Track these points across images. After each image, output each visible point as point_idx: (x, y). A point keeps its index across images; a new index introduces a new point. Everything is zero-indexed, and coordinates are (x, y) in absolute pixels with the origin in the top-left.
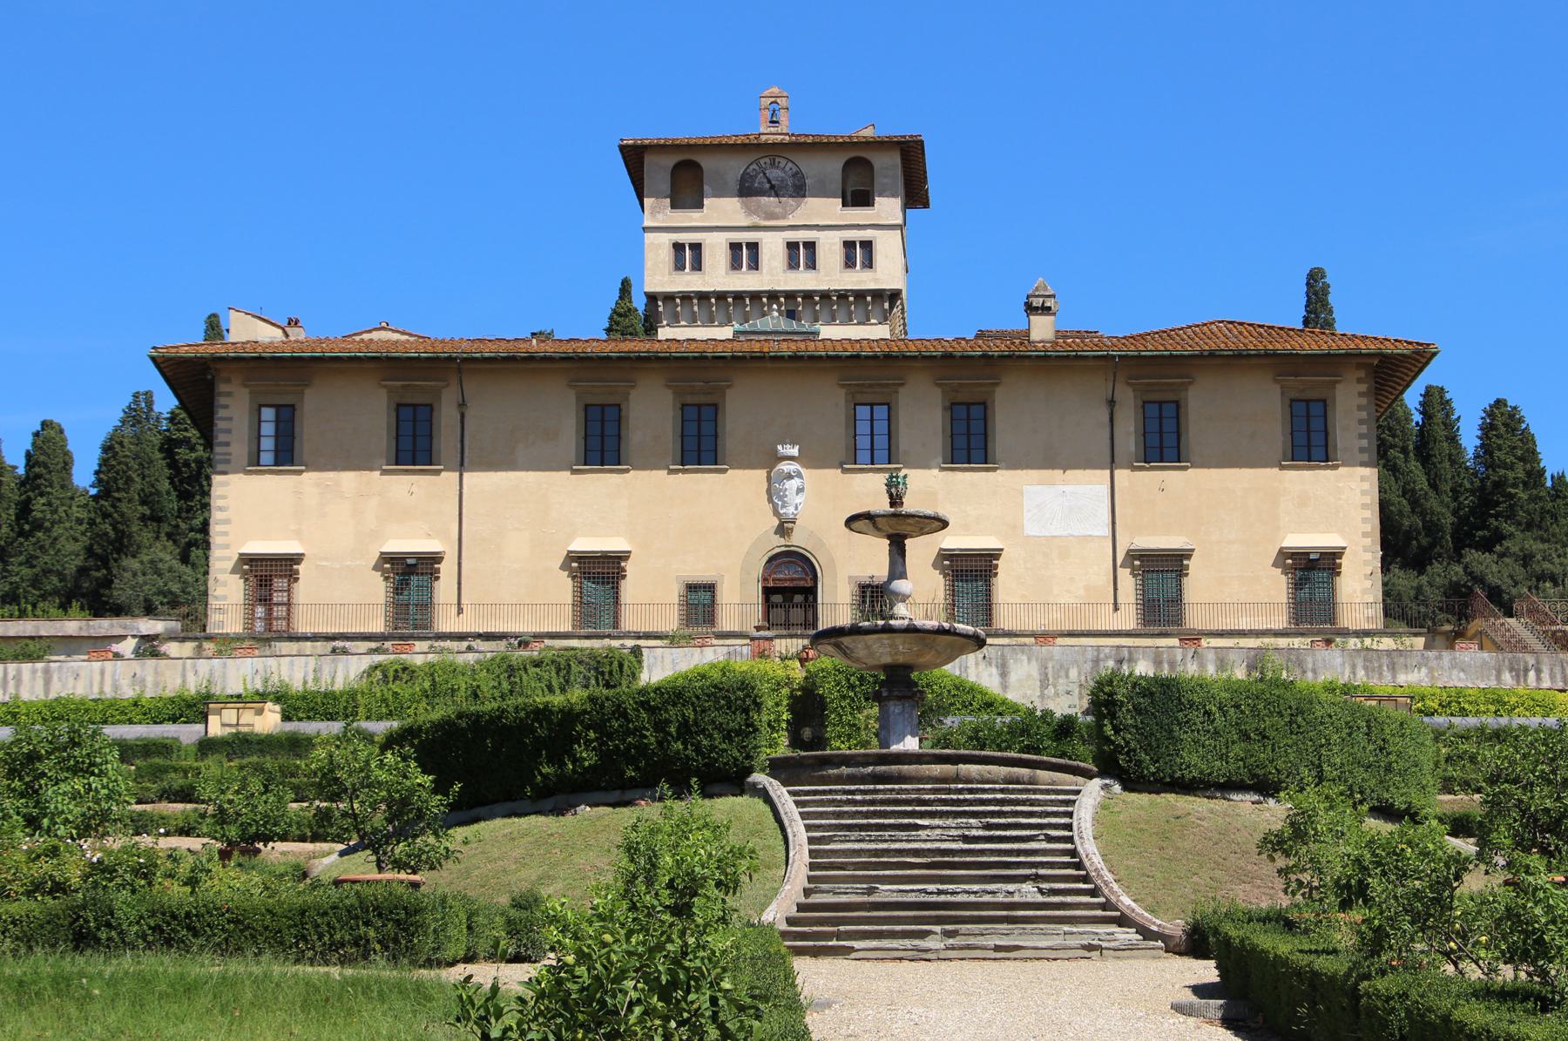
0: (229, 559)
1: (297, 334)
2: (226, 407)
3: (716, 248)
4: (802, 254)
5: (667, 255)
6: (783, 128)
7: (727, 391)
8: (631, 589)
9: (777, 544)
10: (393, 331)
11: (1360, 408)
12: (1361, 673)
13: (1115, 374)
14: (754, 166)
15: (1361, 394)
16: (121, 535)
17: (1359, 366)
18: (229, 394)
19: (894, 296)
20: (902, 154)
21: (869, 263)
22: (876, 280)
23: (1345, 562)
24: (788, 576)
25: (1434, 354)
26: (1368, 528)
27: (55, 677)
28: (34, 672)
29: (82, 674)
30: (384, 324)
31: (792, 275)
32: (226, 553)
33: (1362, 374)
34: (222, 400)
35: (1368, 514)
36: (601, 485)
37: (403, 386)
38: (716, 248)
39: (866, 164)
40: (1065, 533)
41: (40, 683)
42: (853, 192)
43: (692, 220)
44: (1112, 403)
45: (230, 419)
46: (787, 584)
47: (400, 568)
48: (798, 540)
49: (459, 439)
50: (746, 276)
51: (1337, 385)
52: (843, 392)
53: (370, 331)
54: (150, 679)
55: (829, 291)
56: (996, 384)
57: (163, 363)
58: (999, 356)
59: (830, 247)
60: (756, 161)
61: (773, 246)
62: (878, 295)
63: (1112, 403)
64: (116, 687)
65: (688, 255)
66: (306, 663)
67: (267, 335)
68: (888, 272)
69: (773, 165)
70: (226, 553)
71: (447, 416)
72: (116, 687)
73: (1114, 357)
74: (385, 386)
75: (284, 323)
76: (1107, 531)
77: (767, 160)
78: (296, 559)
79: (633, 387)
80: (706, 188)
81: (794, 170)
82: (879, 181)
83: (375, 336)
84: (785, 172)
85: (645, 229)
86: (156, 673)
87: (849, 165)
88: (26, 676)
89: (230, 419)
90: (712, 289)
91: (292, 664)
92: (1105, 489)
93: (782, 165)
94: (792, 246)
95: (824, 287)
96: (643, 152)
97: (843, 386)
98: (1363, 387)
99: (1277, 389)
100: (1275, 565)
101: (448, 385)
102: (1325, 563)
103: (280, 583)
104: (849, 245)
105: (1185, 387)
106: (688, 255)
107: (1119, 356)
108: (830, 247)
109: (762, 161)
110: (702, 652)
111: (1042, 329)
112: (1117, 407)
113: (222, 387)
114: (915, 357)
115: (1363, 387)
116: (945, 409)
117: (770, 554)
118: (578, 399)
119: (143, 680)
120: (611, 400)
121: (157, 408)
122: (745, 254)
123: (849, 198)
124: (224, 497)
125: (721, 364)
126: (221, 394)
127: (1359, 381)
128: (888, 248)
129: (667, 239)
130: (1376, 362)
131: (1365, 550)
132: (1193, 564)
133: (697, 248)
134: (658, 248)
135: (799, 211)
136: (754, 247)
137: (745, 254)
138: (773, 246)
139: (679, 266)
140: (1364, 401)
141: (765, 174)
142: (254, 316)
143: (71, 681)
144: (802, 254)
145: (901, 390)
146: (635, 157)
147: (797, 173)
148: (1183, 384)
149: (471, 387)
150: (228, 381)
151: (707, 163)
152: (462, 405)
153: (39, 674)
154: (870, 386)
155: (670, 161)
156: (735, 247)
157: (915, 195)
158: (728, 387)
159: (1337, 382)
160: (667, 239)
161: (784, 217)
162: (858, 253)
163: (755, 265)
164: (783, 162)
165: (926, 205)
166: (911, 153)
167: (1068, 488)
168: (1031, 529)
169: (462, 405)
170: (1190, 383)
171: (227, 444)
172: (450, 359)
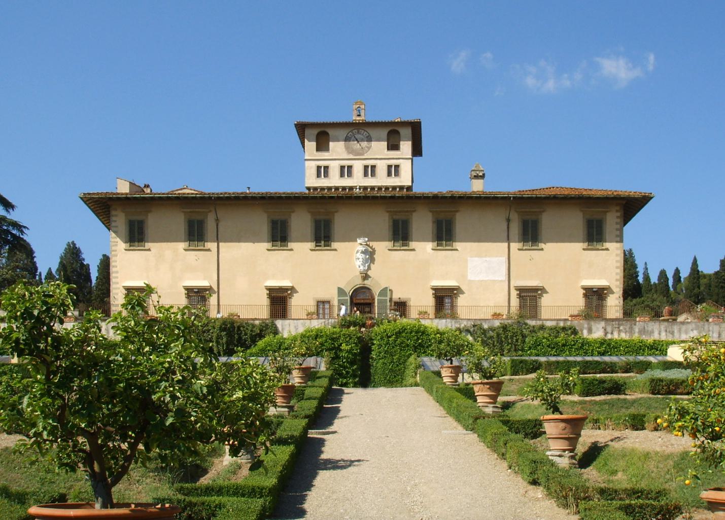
2: (115, 221)
4: (370, 171)
5: (314, 171)
6: (362, 118)
7: (336, 214)
9: (358, 282)
10: (191, 190)
11: (617, 223)
12: (663, 334)
13: (510, 210)
14: (350, 133)
15: (618, 217)
17: (617, 205)
18: (116, 216)
19: (409, 188)
20: (412, 129)
22: (401, 182)
24: (361, 298)
25: (652, 198)
30: (185, 187)
31: (366, 179)
33: (618, 208)
34: (113, 218)
36: (280, 256)
37: (190, 212)
39: (397, 133)
40: (487, 279)
42: (392, 145)
43: (324, 156)
44: (508, 220)
45: (116, 227)
46: (362, 301)
48: (367, 283)
49: (216, 235)
50: (347, 180)
51: (607, 213)
52: (387, 214)
53: (181, 189)
55: (382, 186)
56: (457, 211)
57: (87, 201)
58: (459, 197)
59: (382, 167)
61: (358, 167)
62: (401, 188)
65: (322, 171)
69: (358, 133)
73: (511, 197)
74: (183, 212)
75: (142, 186)
77: (356, 131)
79: (293, 212)
81: (367, 134)
84: (364, 136)
85: (306, 160)
89: (116, 227)
90: (333, 185)
92: (504, 259)
93: (362, 133)
94: (366, 167)
95: (380, 184)
96: (304, 128)
97: (388, 212)
98: (619, 214)
101: (210, 211)
105: (541, 212)
107: (513, 197)
108: (382, 167)
109: (354, 131)
110: (311, 322)
111: (477, 186)
112: (510, 223)
113: (113, 213)
114: (421, 197)
115: (619, 214)
116: (434, 222)
117: (354, 288)
118: (268, 217)
122: (347, 171)
123: (390, 147)
126: (112, 216)
127: (617, 211)
130: (624, 202)
133: (326, 168)
134: (310, 168)
135: (369, 152)
136: (350, 167)
138: (358, 167)
139: (319, 175)
140: (619, 220)
141: (355, 137)
144: (370, 171)
145: (414, 214)
146: (302, 129)
147: (368, 136)
148: (540, 212)
149: (221, 213)
150: (116, 210)
151: (331, 132)
152: (217, 220)
154: (400, 212)
155: (315, 132)
157: (417, 151)
158: (336, 212)
159: (607, 212)
160: (314, 164)
161: (363, 155)
162: (393, 170)
164: (363, 131)
165: (421, 155)
166: (416, 129)
167: (488, 259)
169: (217, 220)
170: (543, 211)
172: (210, 198)
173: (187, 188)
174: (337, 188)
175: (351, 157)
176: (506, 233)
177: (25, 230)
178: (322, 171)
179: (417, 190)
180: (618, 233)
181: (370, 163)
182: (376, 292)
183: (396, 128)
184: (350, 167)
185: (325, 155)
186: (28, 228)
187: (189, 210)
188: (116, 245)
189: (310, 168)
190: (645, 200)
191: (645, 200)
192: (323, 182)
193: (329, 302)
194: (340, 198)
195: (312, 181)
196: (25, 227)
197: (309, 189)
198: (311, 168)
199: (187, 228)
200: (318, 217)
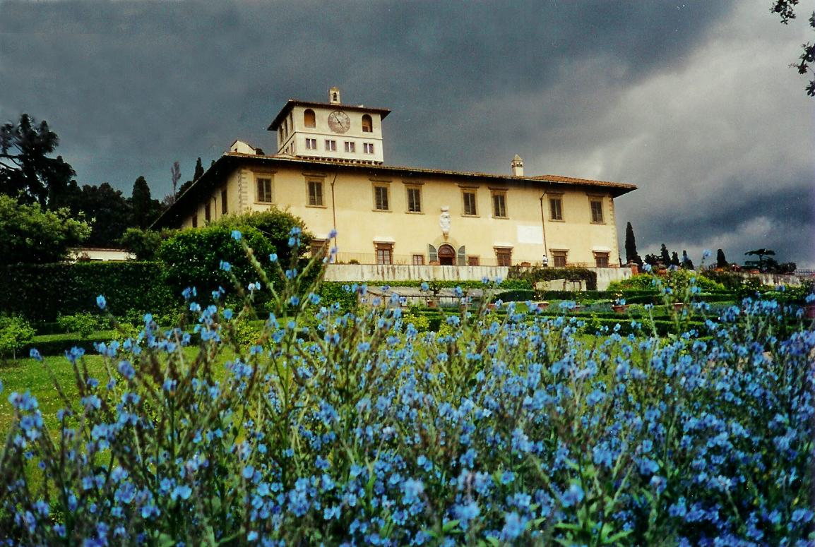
4: (350, 146)
5: (304, 142)
9: (442, 242)
19: (381, 163)
28: (388, 269)
35: (615, 240)
44: (541, 199)
48: (449, 242)
54: (431, 274)
63: (541, 199)
76: (542, 242)
80: (316, 120)
88: (385, 271)
120: (384, 186)
137: (331, 144)
143: (402, 272)
151: (317, 112)
152: (332, 185)
161: (343, 133)
168: (520, 241)
169: (332, 185)
171: (246, 193)
175: (334, 133)
178: (312, 143)
179: (385, 166)
181: (350, 140)
184: (333, 142)
185: (313, 130)
189: (300, 139)
193: (422, 256)
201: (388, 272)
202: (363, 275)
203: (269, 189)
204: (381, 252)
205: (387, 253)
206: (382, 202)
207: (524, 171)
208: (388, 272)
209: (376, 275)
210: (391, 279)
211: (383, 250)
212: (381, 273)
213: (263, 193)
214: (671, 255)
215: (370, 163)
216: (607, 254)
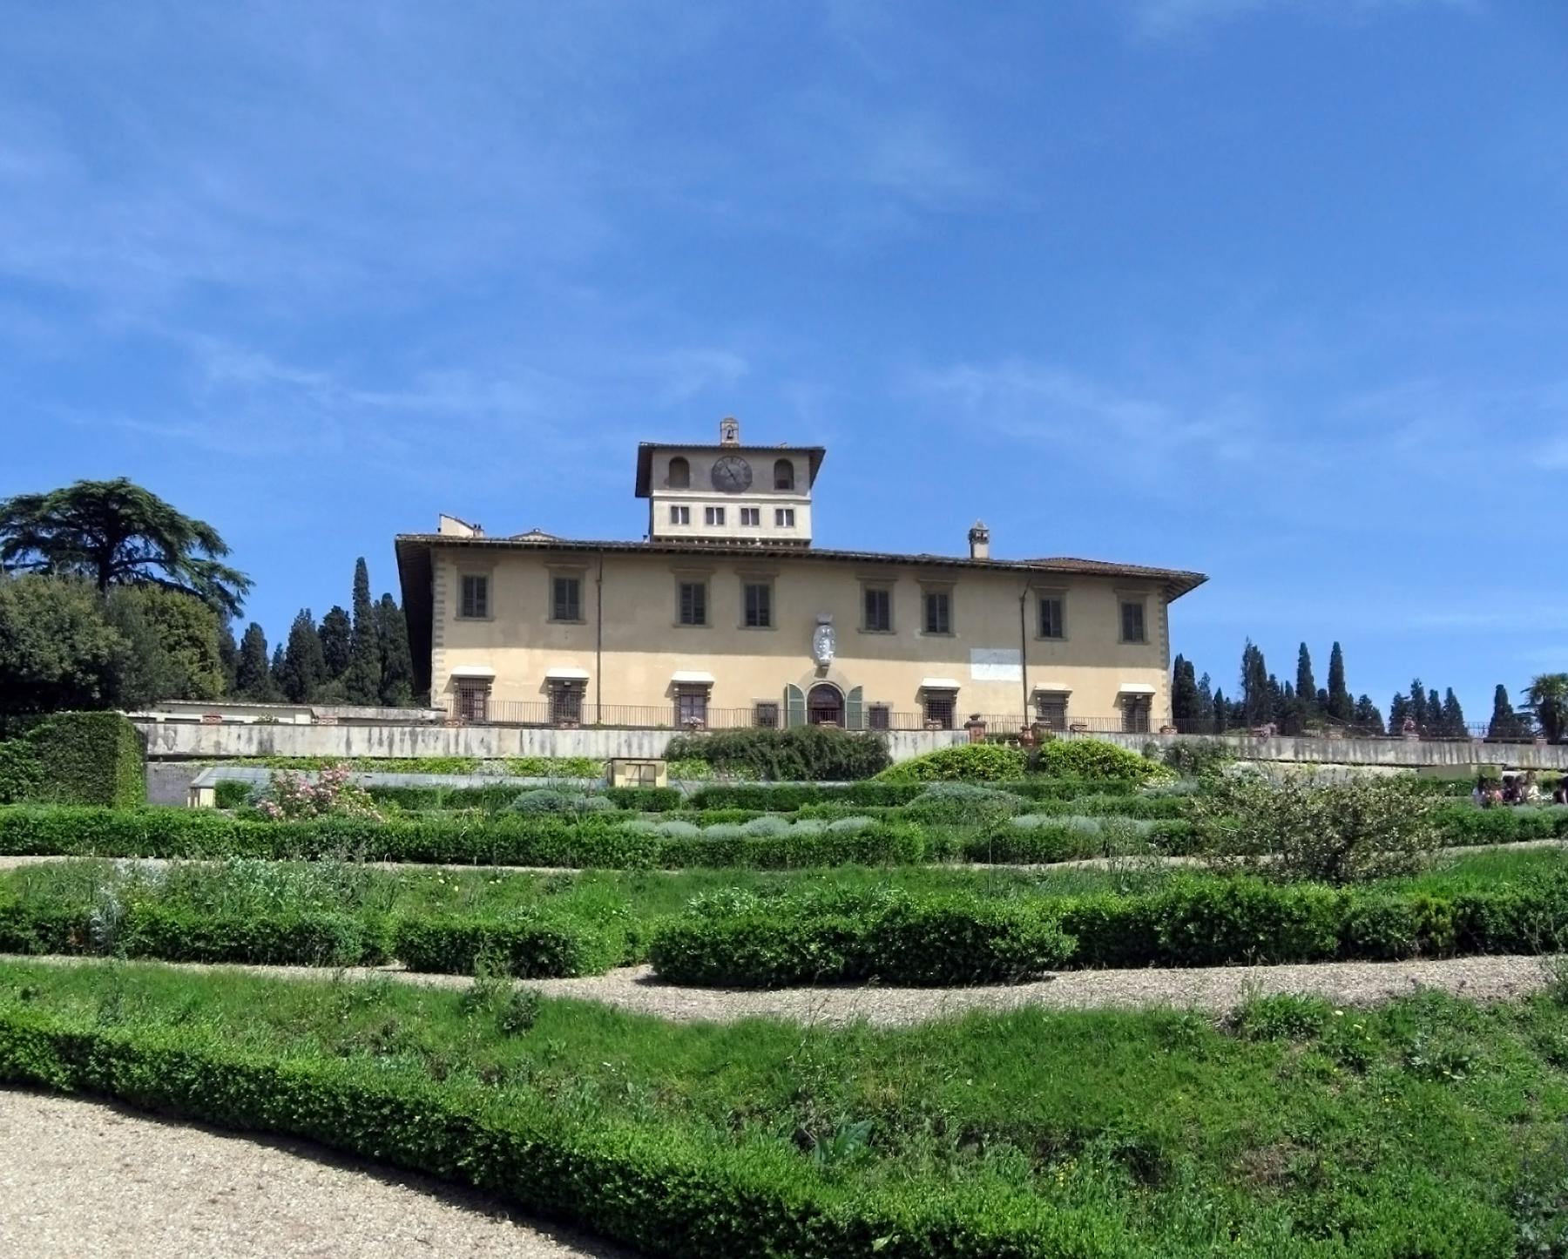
0: (444, 678)
1: (481, 535)
2: (442, 577)
3: (698, 510)
8: (711, 705)
16: (302, 683)
18: (444, 569)
19: (807, 543)
21: (791, 522)
23: (1154, 701)
26: (1165, 682)
27: (420, 738)
28: (403, 734)
29: (441, 737)
32: (443, 673)
38: (698, 510)
41: (408, 743)
45: (444, 586)
47: (558, 688)
54: (494, 745)
59: (767, 512)
60: (722, 459)
61: (733, 511)
62: (797, 542)
64: (467, 747)
66: (619, 736)
67: (464, 533)
68: (802, 529)
70: (443, 673)
71: (588, 590)
72: (467, 747)
76: (1019, 678)
78: (488, 680)
80: (691, 474)
82: (797, 474)
83: (532, 538)
86: (500, 740)
87: (779, 464)
88: (397, 738)
91: (607, 737)
95: (765, 536)
99: (1115, 597)
100: (1115, 706)
102: (1143, 702)
103: (479, 696)
104: (779, 512)
106: (680, 514)
108: (767, 512)
119: (489, 744)
120: (700, 581)
121: (313, 618)
124: (440, 637)
125: (772, 560)
128: (803, 514)
129: (667, 505)
130: (1167, 583)
131: (1164, 694)
132: (1071, 700)
136: (721, 511)
137: (715, 515)
138: (733, 511)
142: (456, 520)
144: (751, 516)
150: (443, 560)
151: (692, 460)
152: (599, 581)
153: (407, 737)
155: (669, 457)
156: (709, 511)
160: (667, 505)
163: (721, 522)
169: (599, 581)
171: (442, 602)
173: (534, 533)
174: (701, 539)
176: (1018, 618)
177: (250, 588)
180: (1161, 623)
181: (749, 505)
182: (846, 690)
183: (787, 457)
186: (253, 584)
187: (557, 565)
188: (443, 613)
189: (662, 509)
190: (1199, 580)
191: (1199, 580)
192: (681, 531)
194: (723, 554)
195: (663, 528)
196: (248, 582)
197: (659, 539)
198: (663, 508)
199: (553, 590)
200: (751, 582)
201: (402, 741)
202: (348, 744)
203: (482, 594)
204: (686, 701)
205: (698, 701)
206: (693, 611)
207: (989, 550)
208: (402, 741)
209: (376, 746)
210: (407, 753)
211: (692, 696)
212: (386, 743)
213: (471, 602)
214: (1427, 695)
215: (753, 541)
216: (1148, 697)
